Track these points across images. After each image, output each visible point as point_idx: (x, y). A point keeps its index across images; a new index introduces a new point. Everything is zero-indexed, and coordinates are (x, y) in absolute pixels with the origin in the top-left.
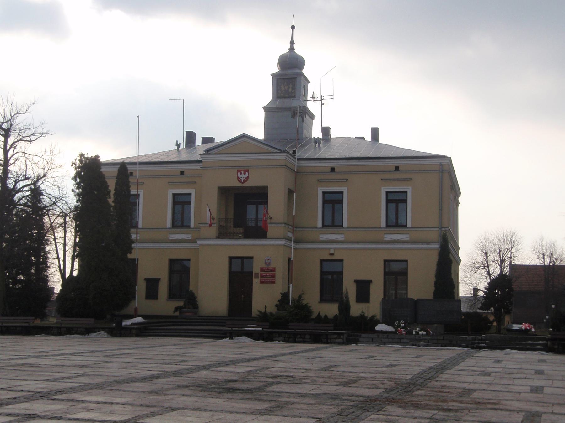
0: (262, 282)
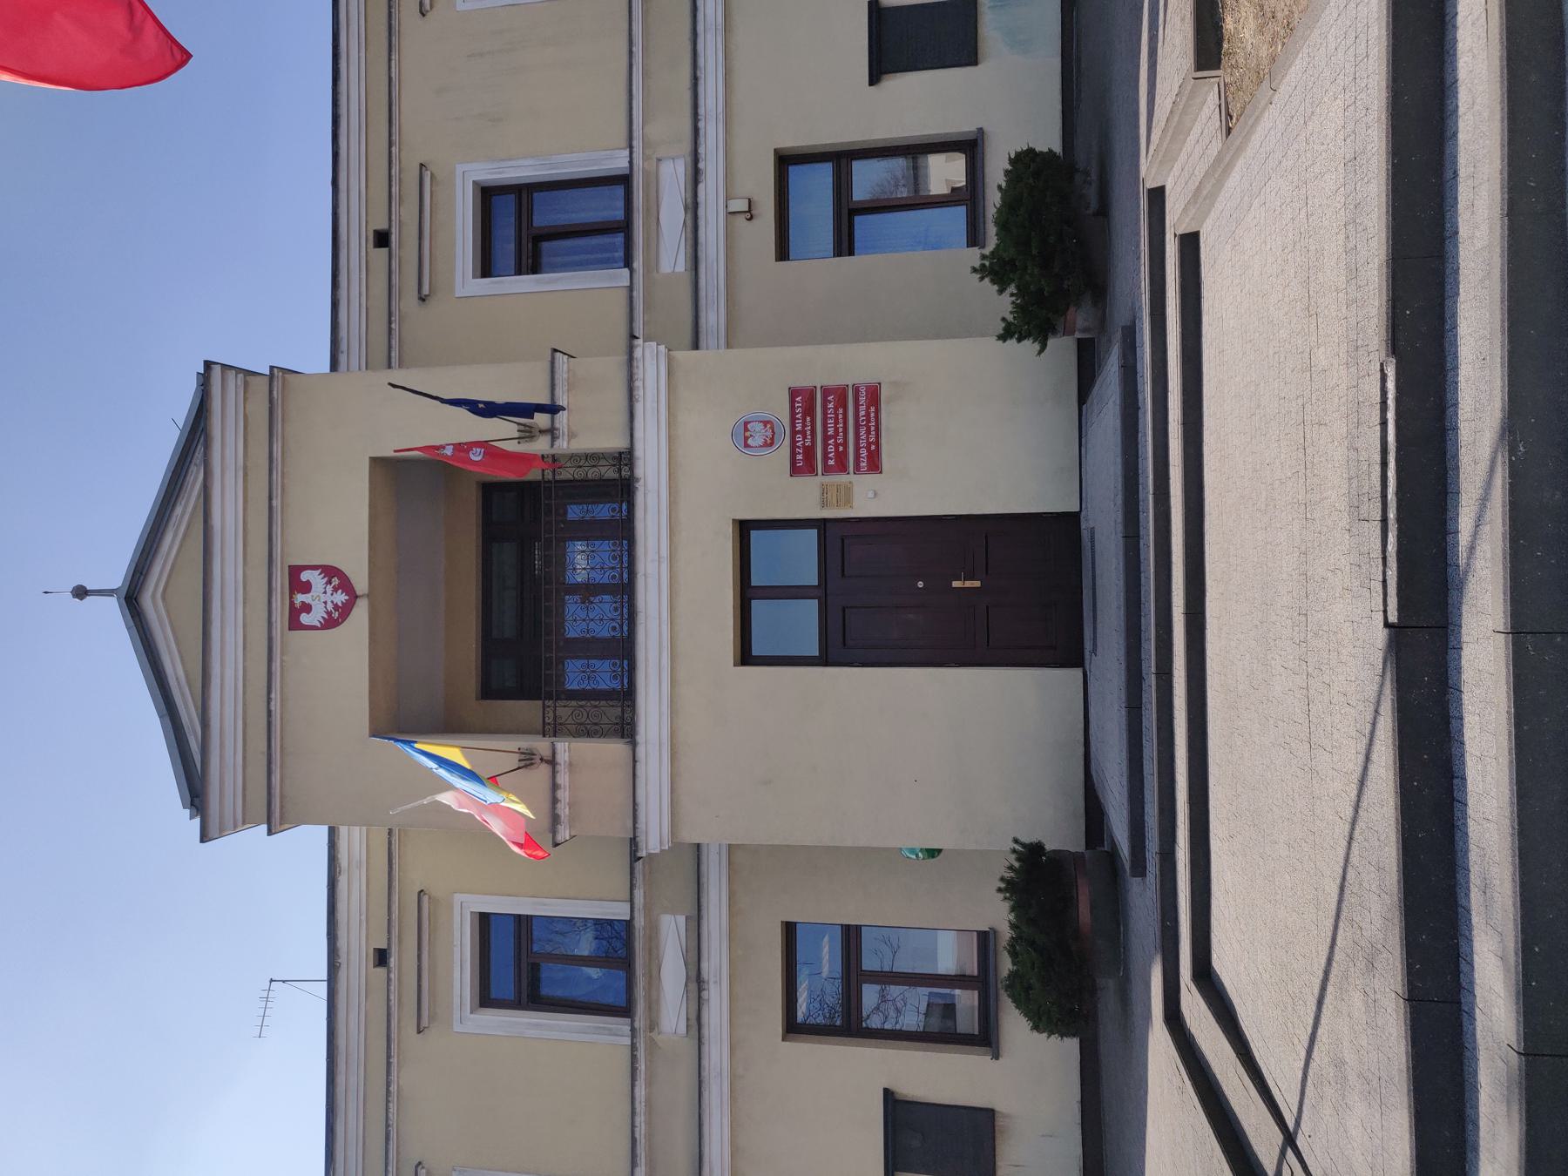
0: (875, 465)
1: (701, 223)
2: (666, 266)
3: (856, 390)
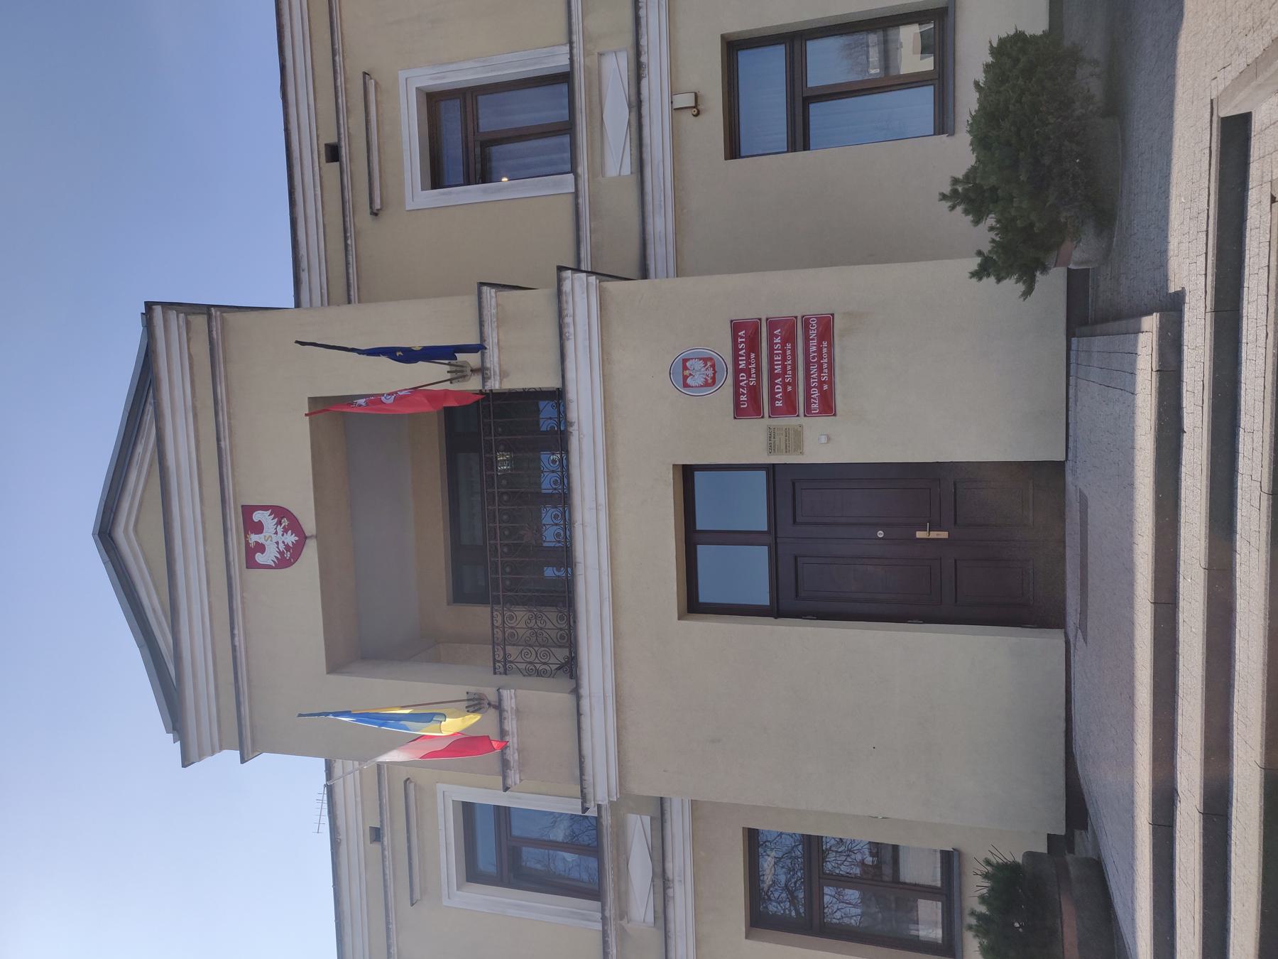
0: (828, 407)
1: (646, 121)
2: (612, 170)
3: (806, 323)
